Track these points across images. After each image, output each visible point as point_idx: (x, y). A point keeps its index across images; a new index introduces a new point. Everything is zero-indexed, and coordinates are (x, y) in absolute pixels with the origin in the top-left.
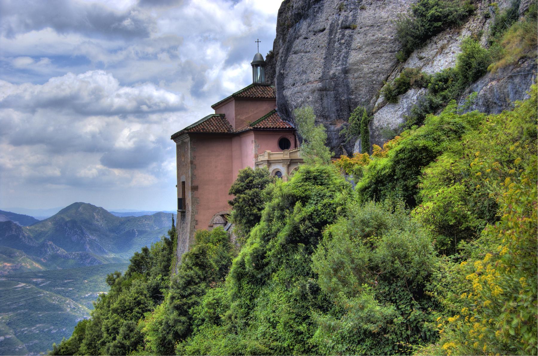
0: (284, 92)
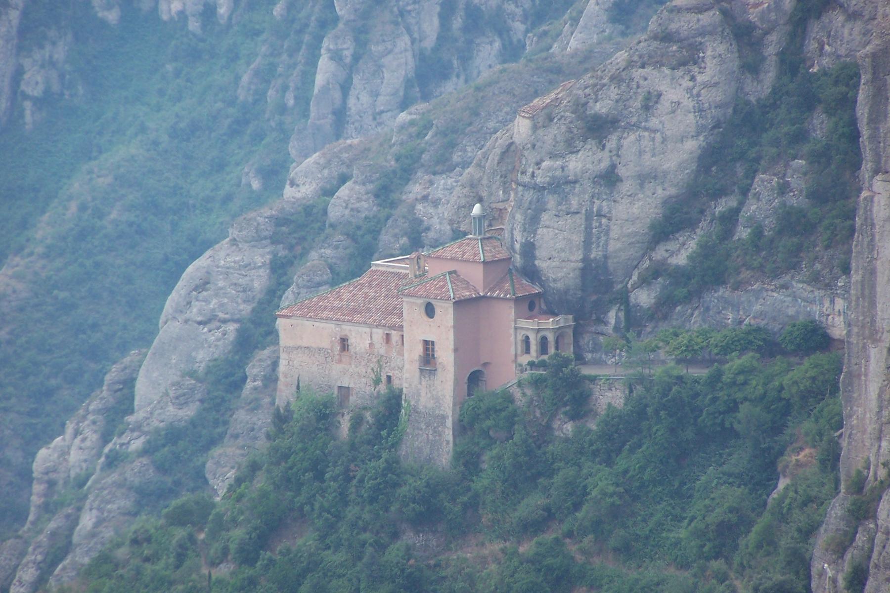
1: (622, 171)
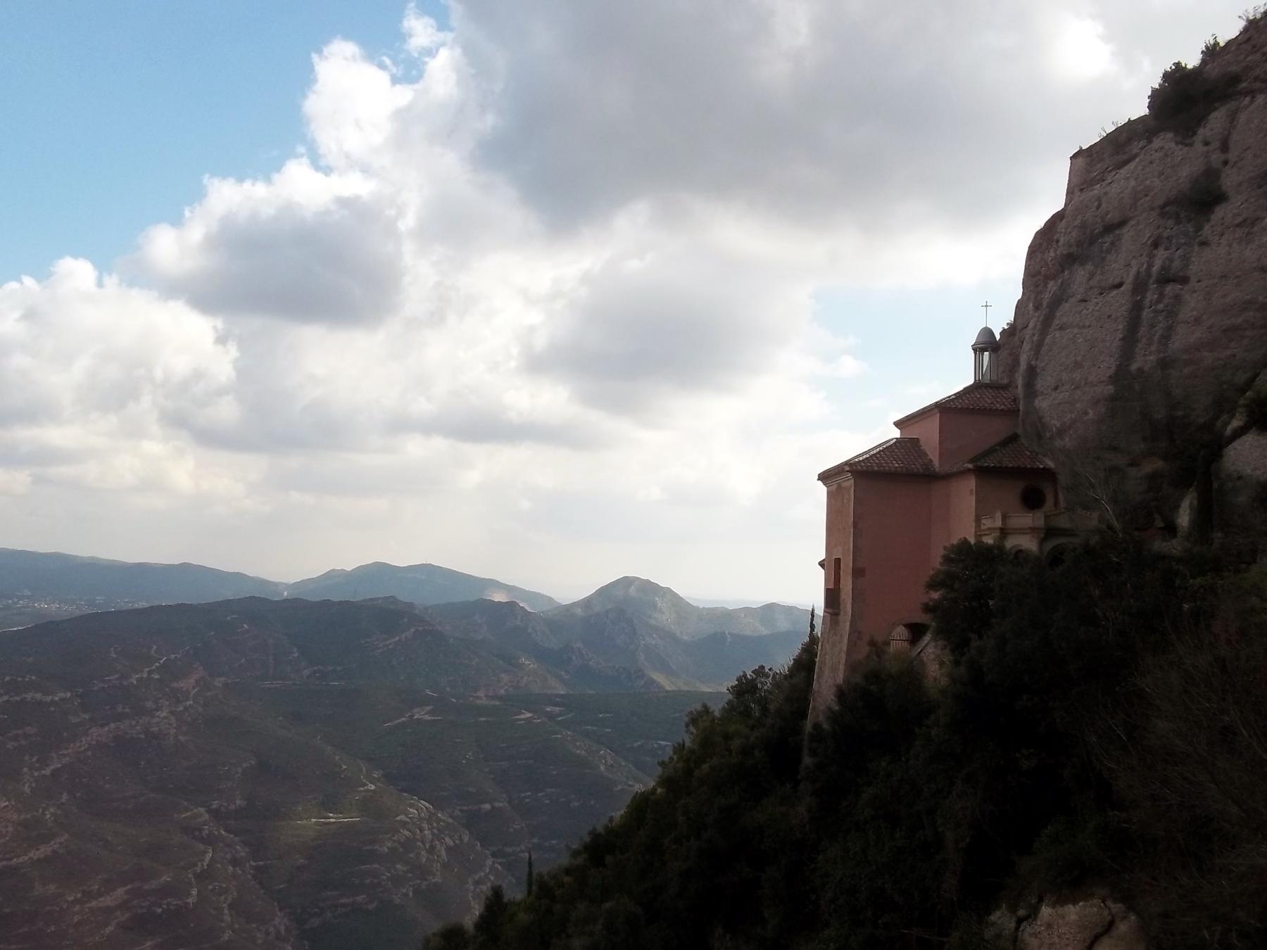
0: (1037, 402)
1: (1229, 180)
